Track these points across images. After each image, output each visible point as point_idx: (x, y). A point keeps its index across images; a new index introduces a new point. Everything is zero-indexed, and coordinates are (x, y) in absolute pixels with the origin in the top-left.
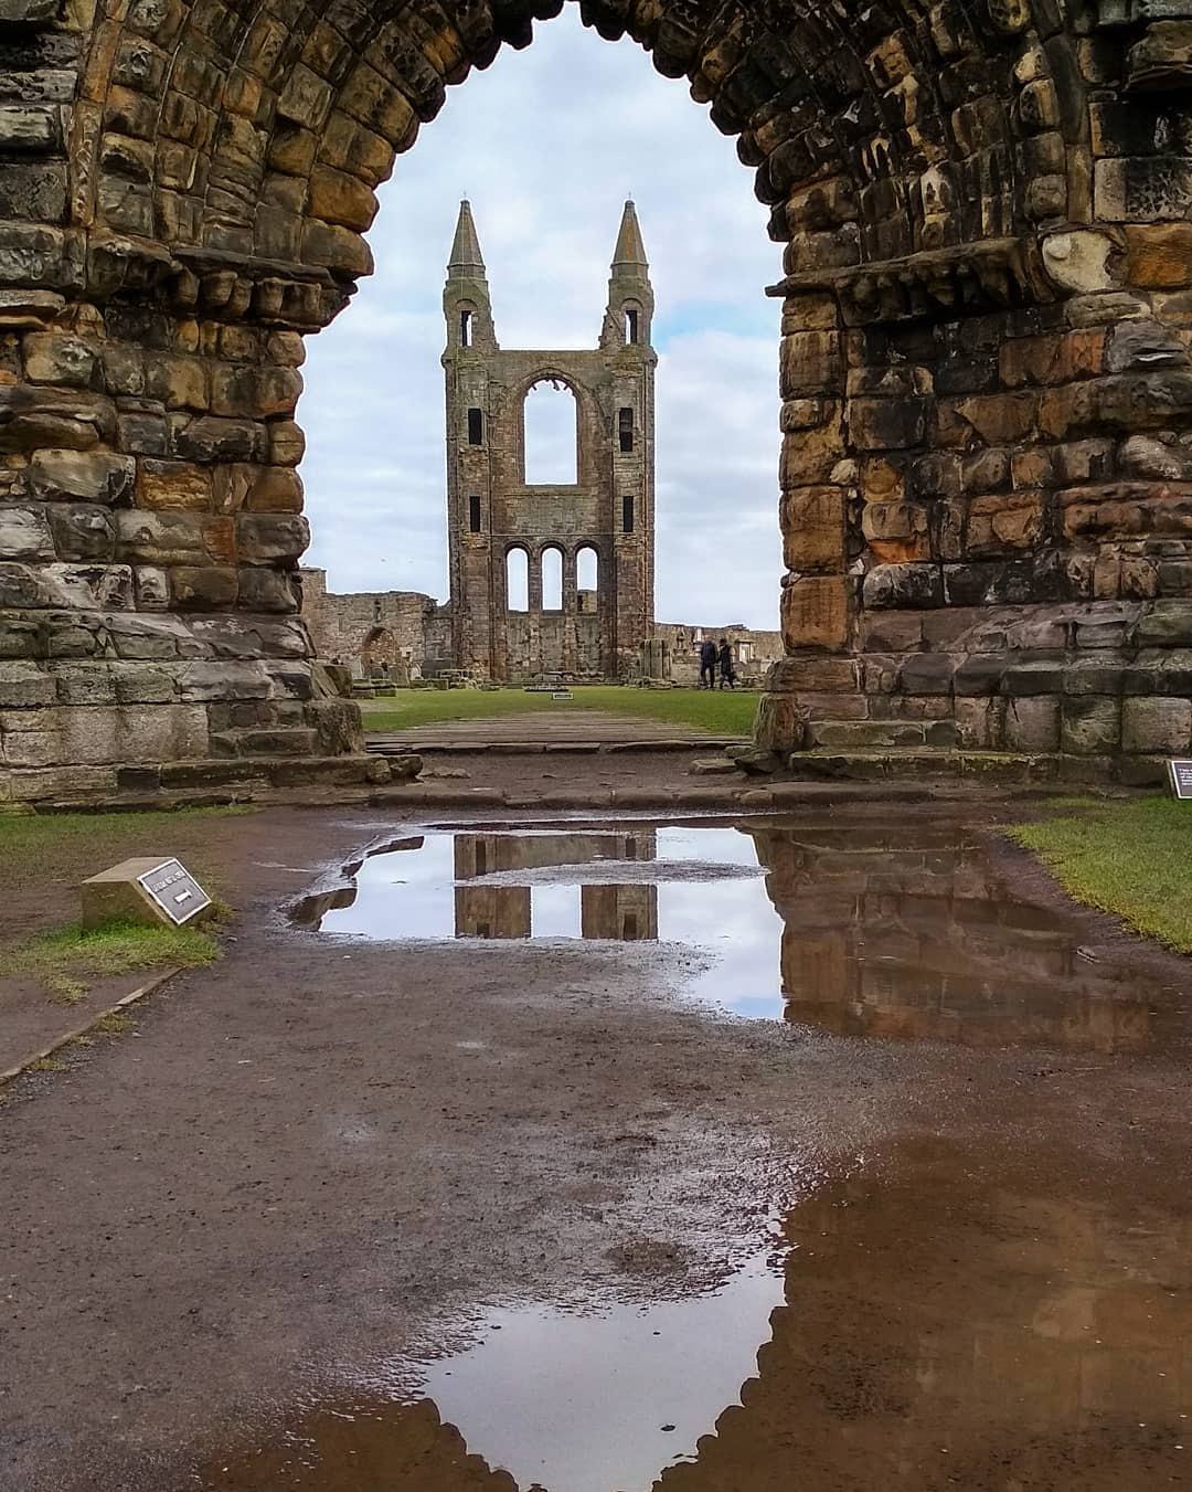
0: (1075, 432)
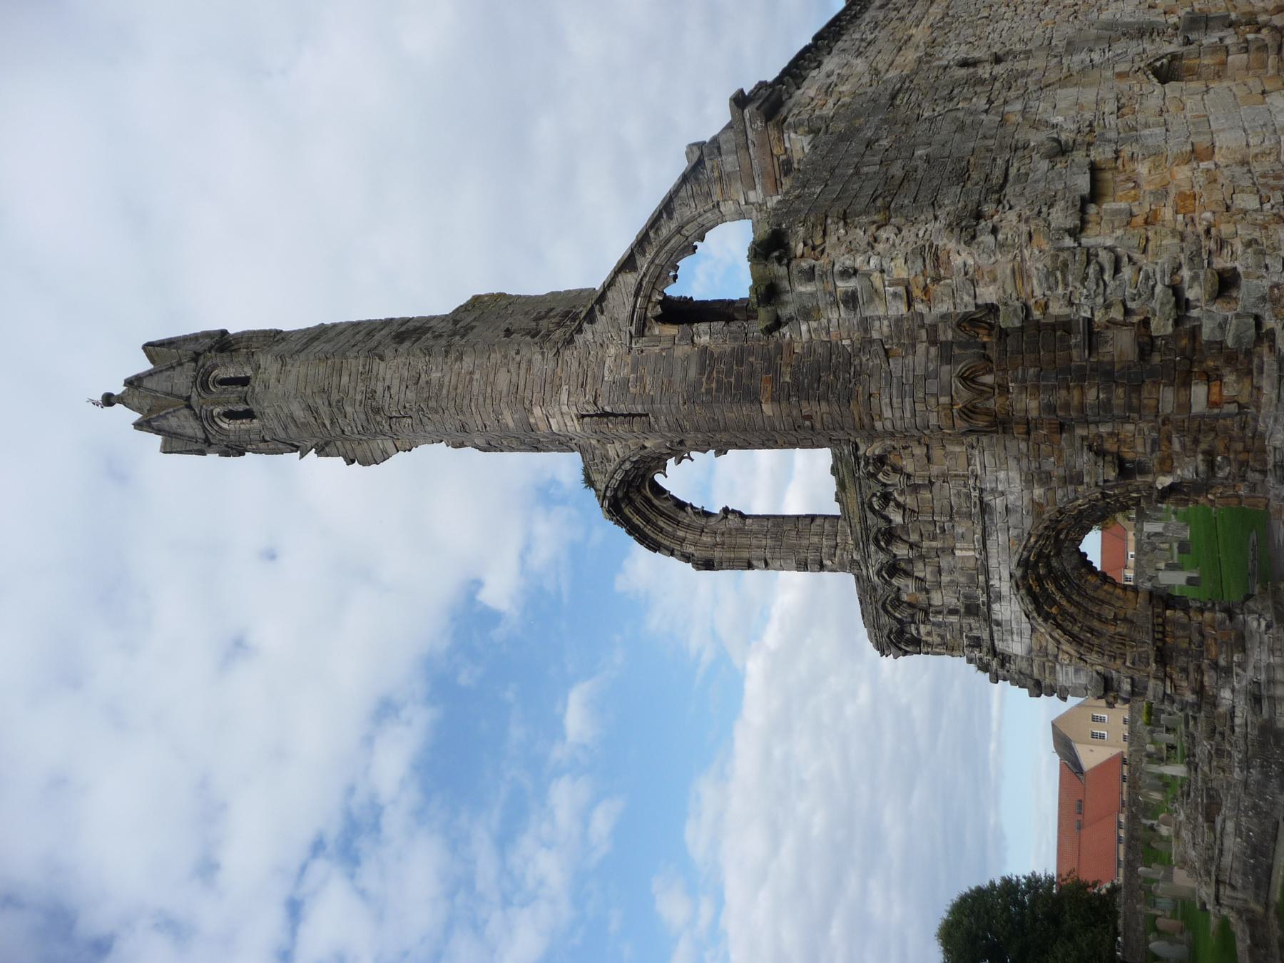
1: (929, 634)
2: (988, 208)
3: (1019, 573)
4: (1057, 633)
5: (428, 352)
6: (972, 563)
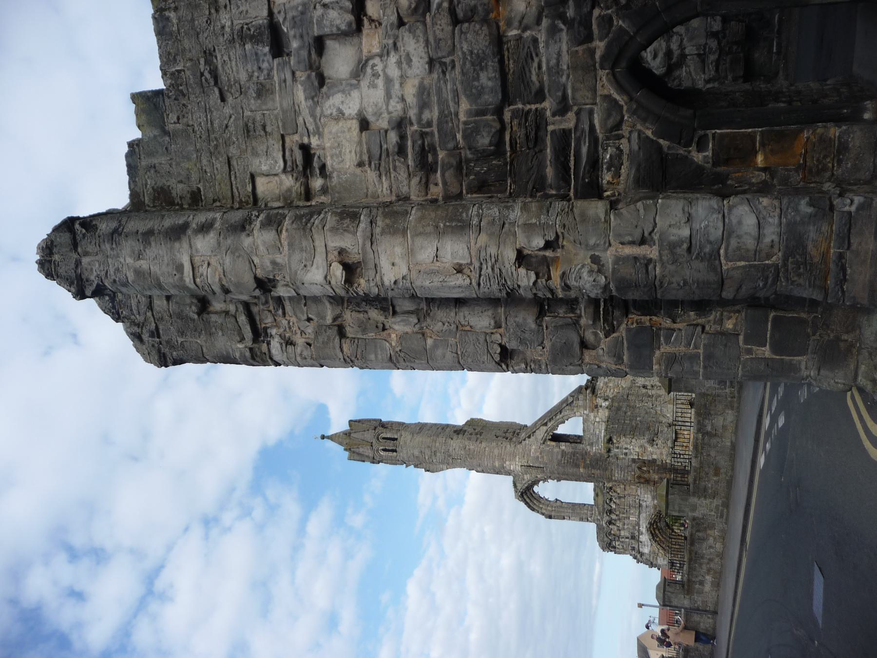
1: (619, 545)
2: (655, 439)
3: (648, 526)
4: (659, 546)
5: (470, 439)
6: (634, 522)
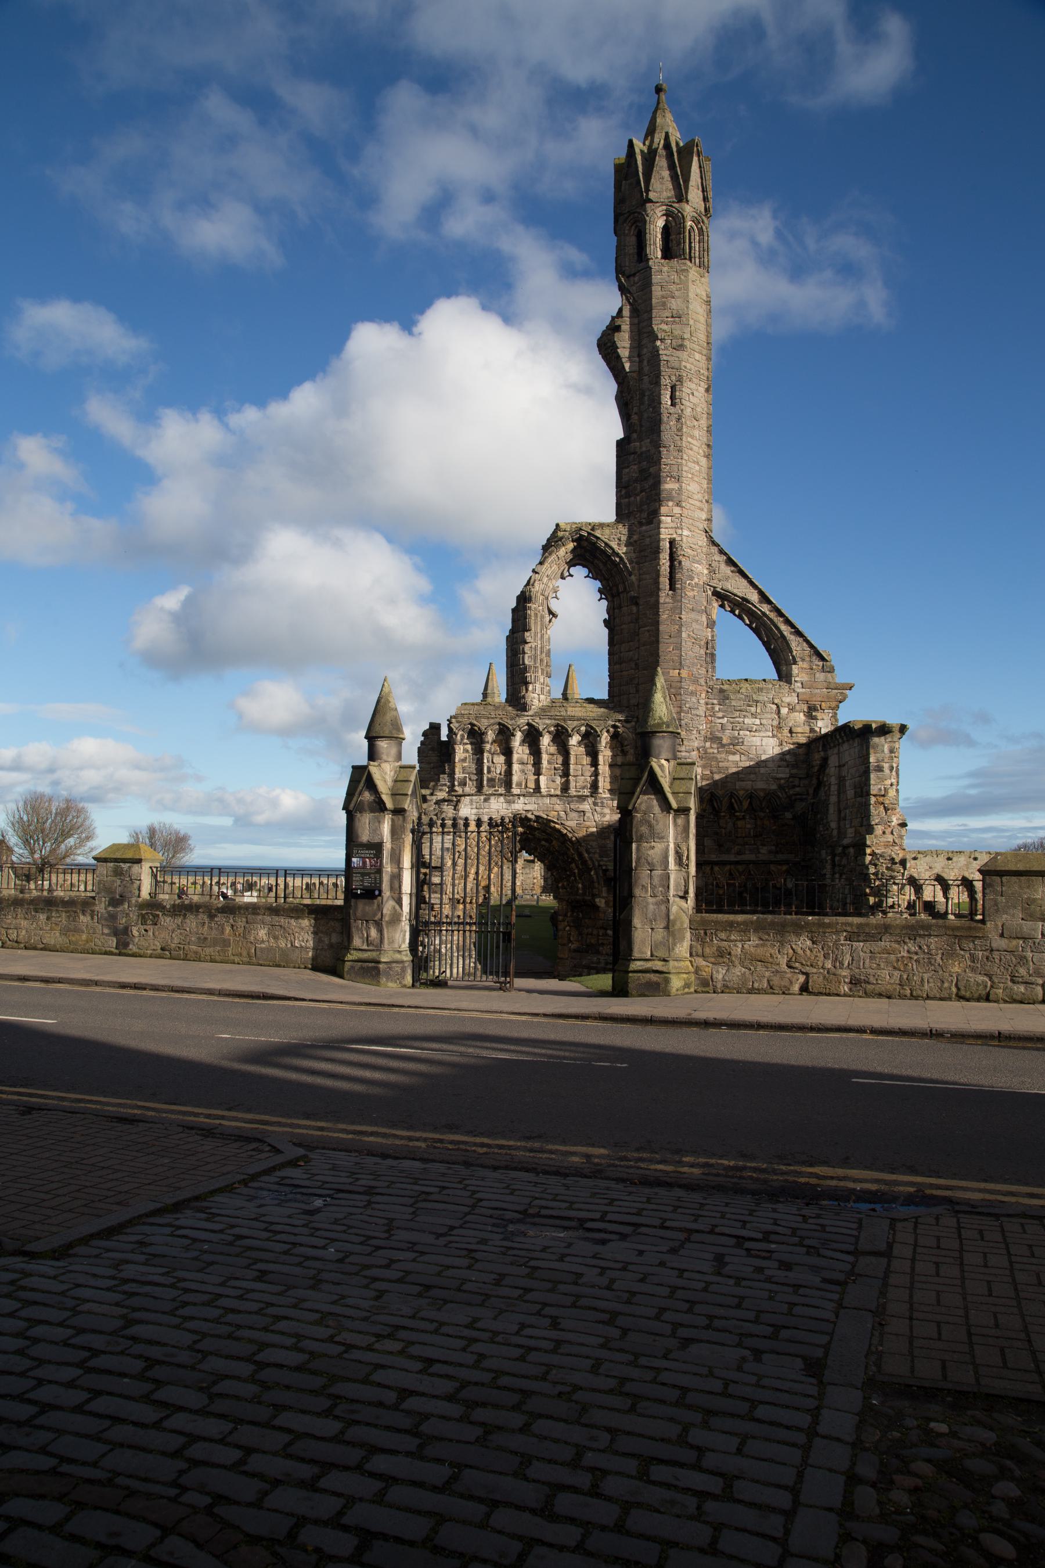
0: (602, 928)
3: (530, 815)
